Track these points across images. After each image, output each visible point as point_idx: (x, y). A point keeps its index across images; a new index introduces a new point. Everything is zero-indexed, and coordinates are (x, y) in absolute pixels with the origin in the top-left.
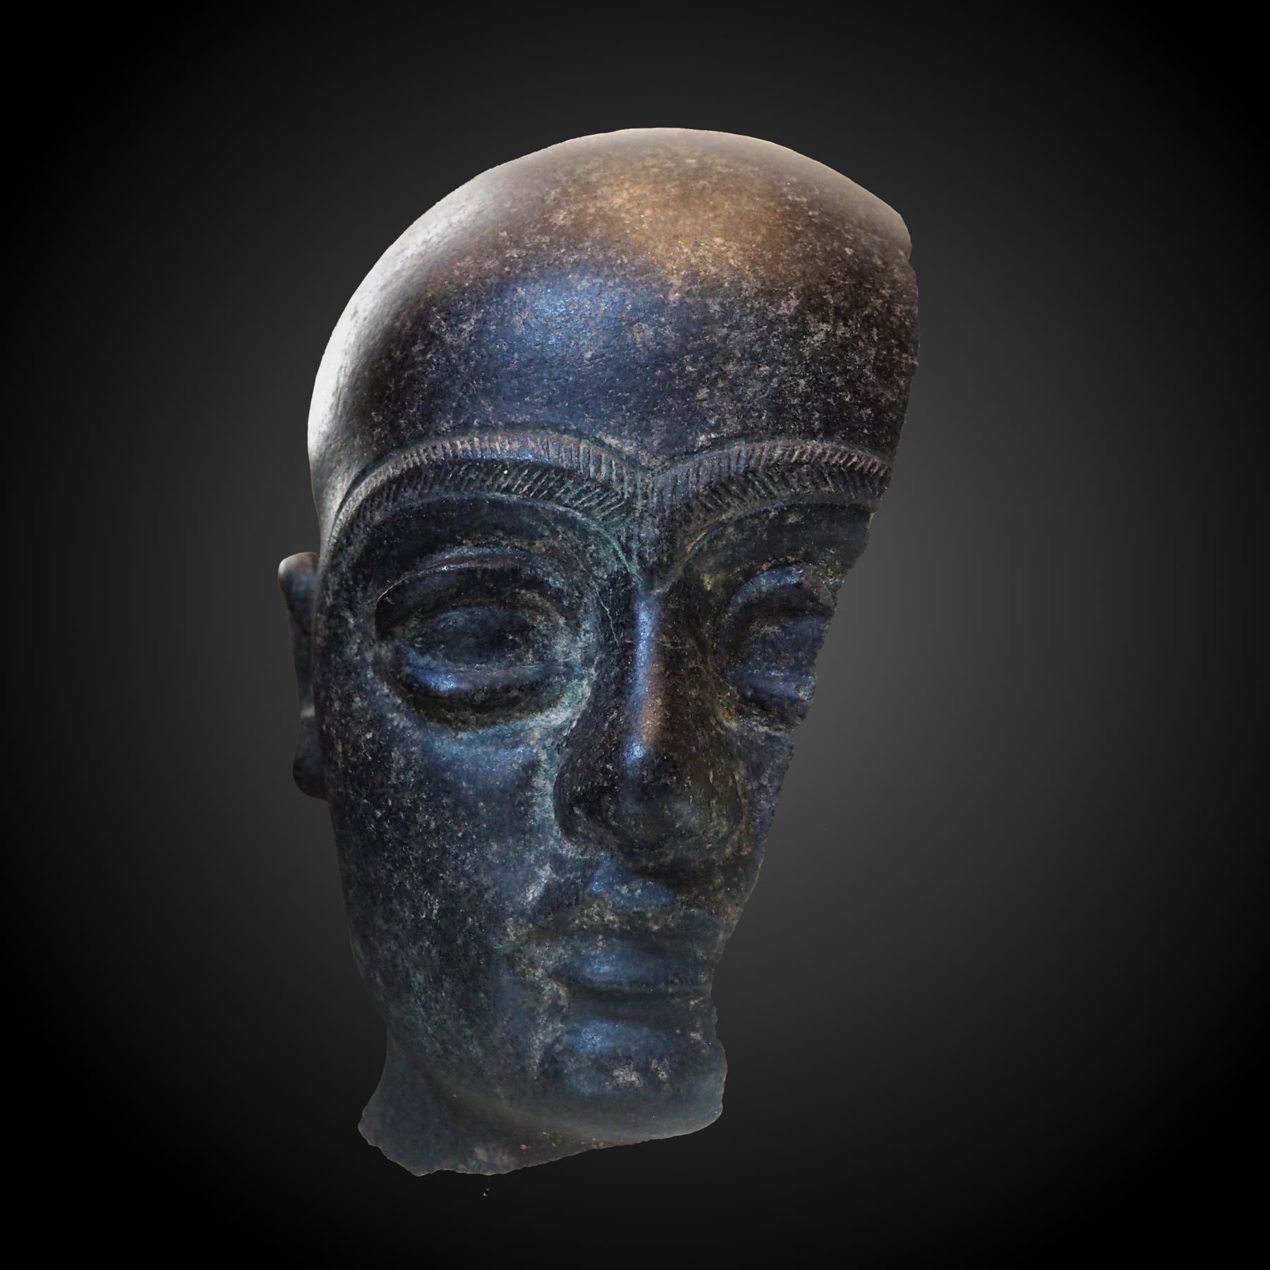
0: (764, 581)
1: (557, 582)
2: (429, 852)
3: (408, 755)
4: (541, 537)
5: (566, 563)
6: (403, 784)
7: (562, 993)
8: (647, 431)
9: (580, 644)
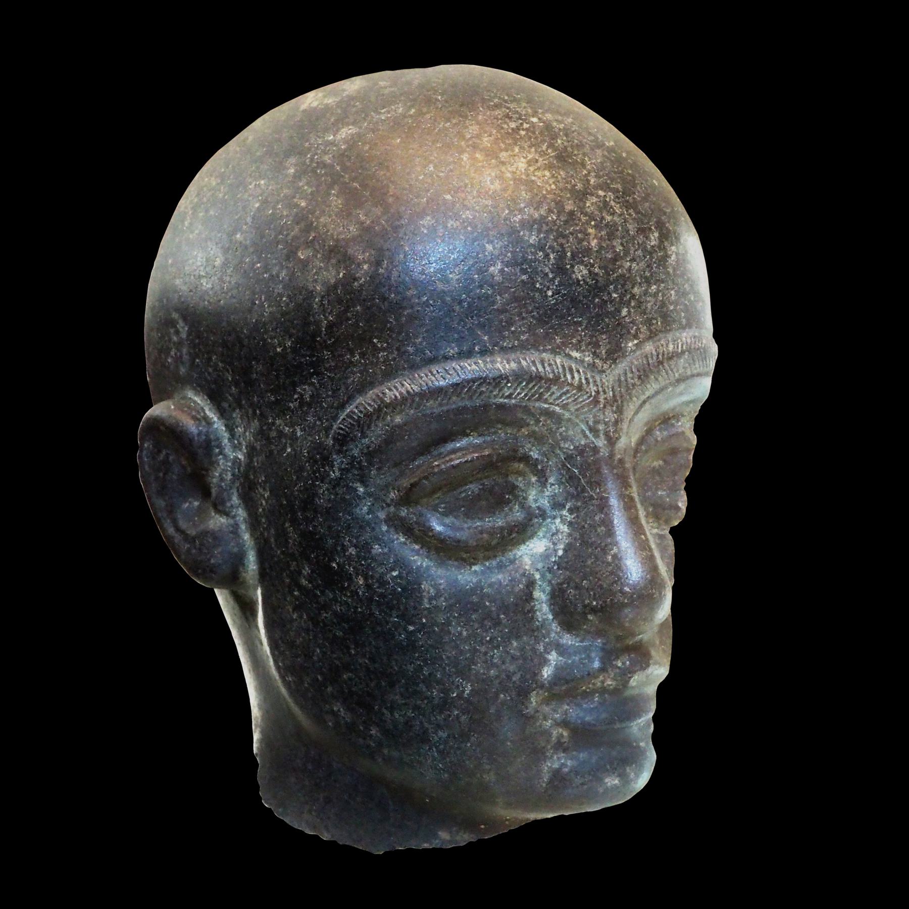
0: (658, 433)
1: (535, 454)
2: (461, 652)
3: (436, 586)
4: (528, 425)
5: (538, 439)
6: (436, 607)
7: (565, 734)
8: (597, 345)
9: (547, 493)
